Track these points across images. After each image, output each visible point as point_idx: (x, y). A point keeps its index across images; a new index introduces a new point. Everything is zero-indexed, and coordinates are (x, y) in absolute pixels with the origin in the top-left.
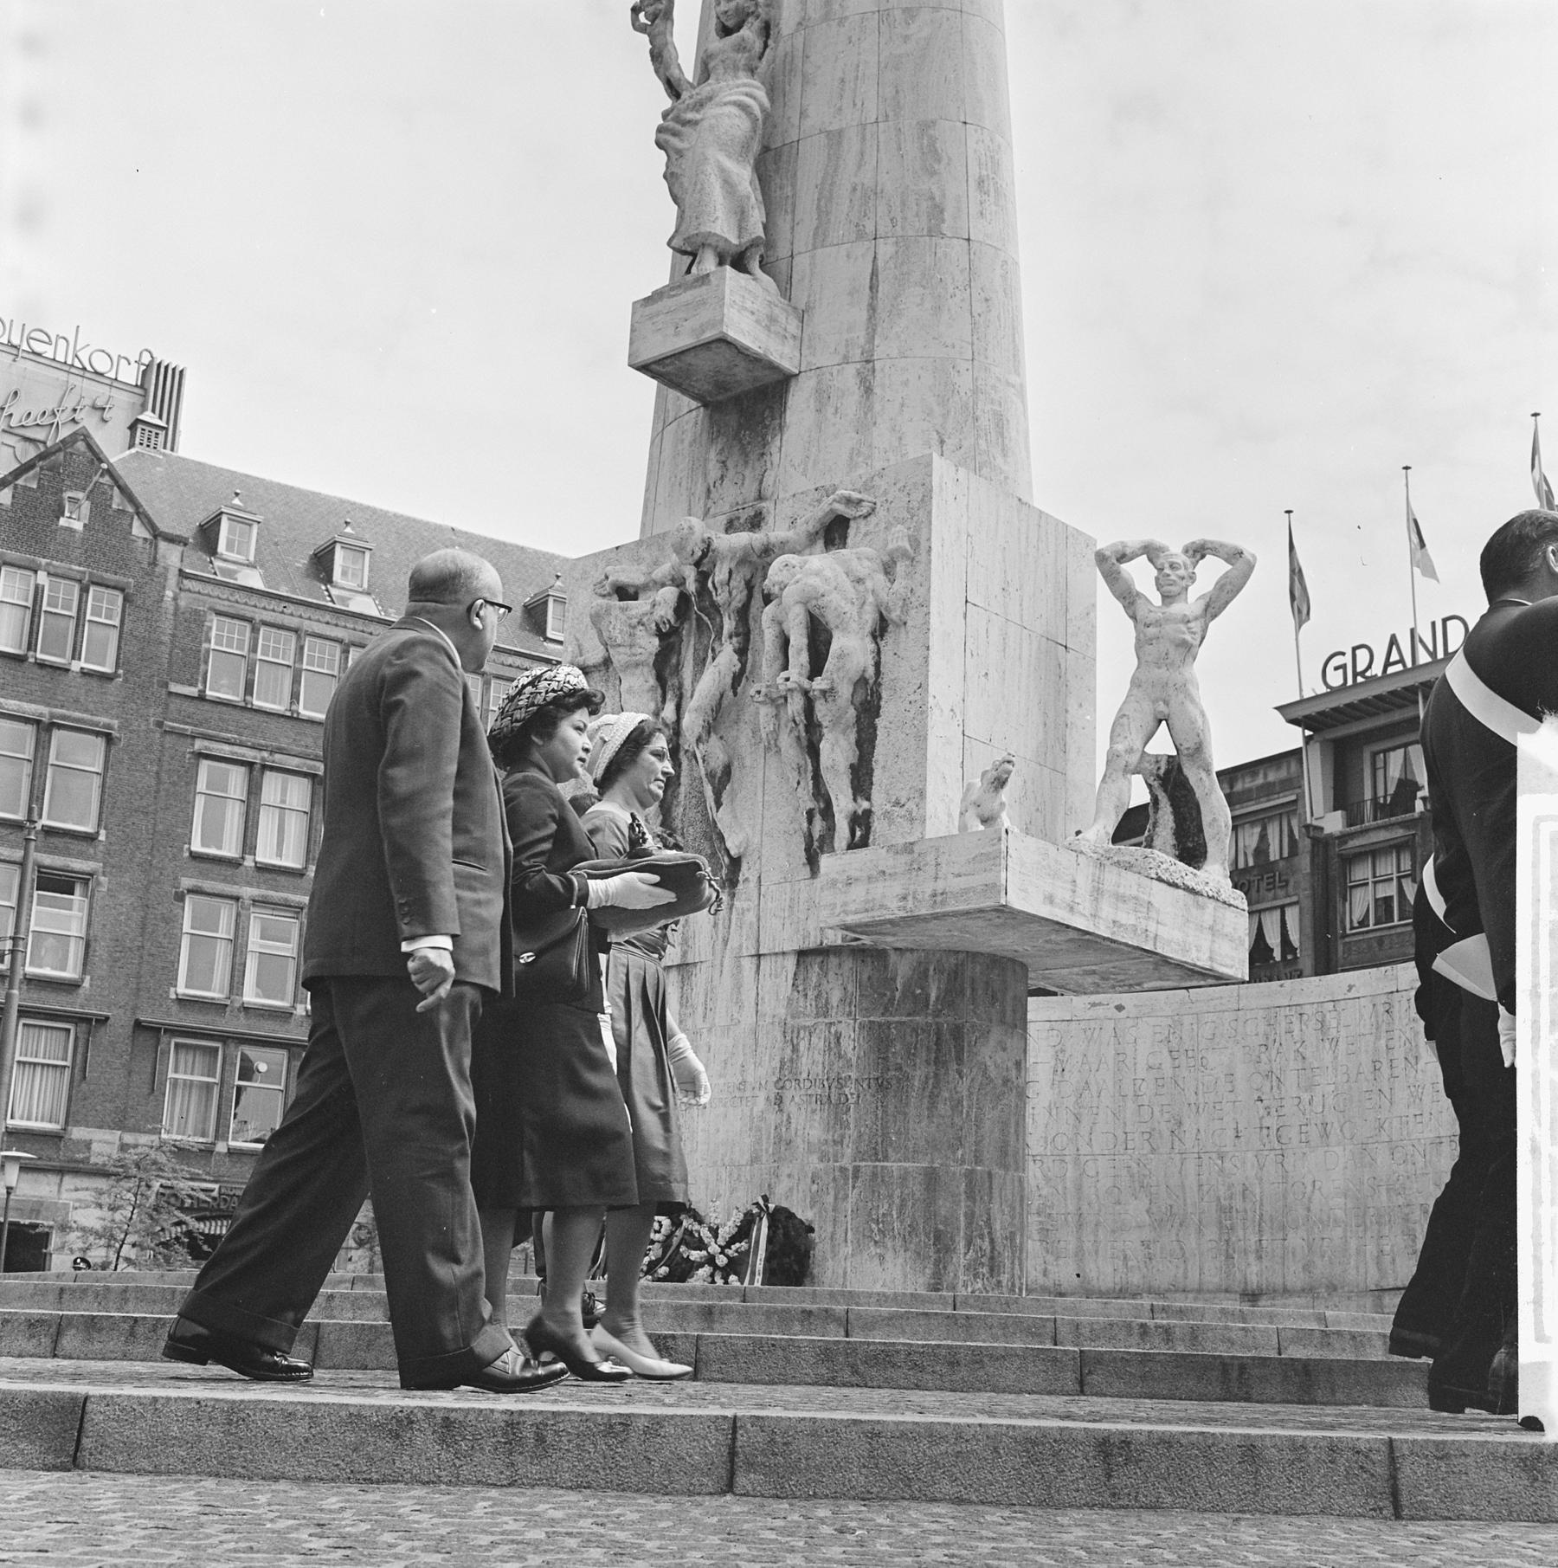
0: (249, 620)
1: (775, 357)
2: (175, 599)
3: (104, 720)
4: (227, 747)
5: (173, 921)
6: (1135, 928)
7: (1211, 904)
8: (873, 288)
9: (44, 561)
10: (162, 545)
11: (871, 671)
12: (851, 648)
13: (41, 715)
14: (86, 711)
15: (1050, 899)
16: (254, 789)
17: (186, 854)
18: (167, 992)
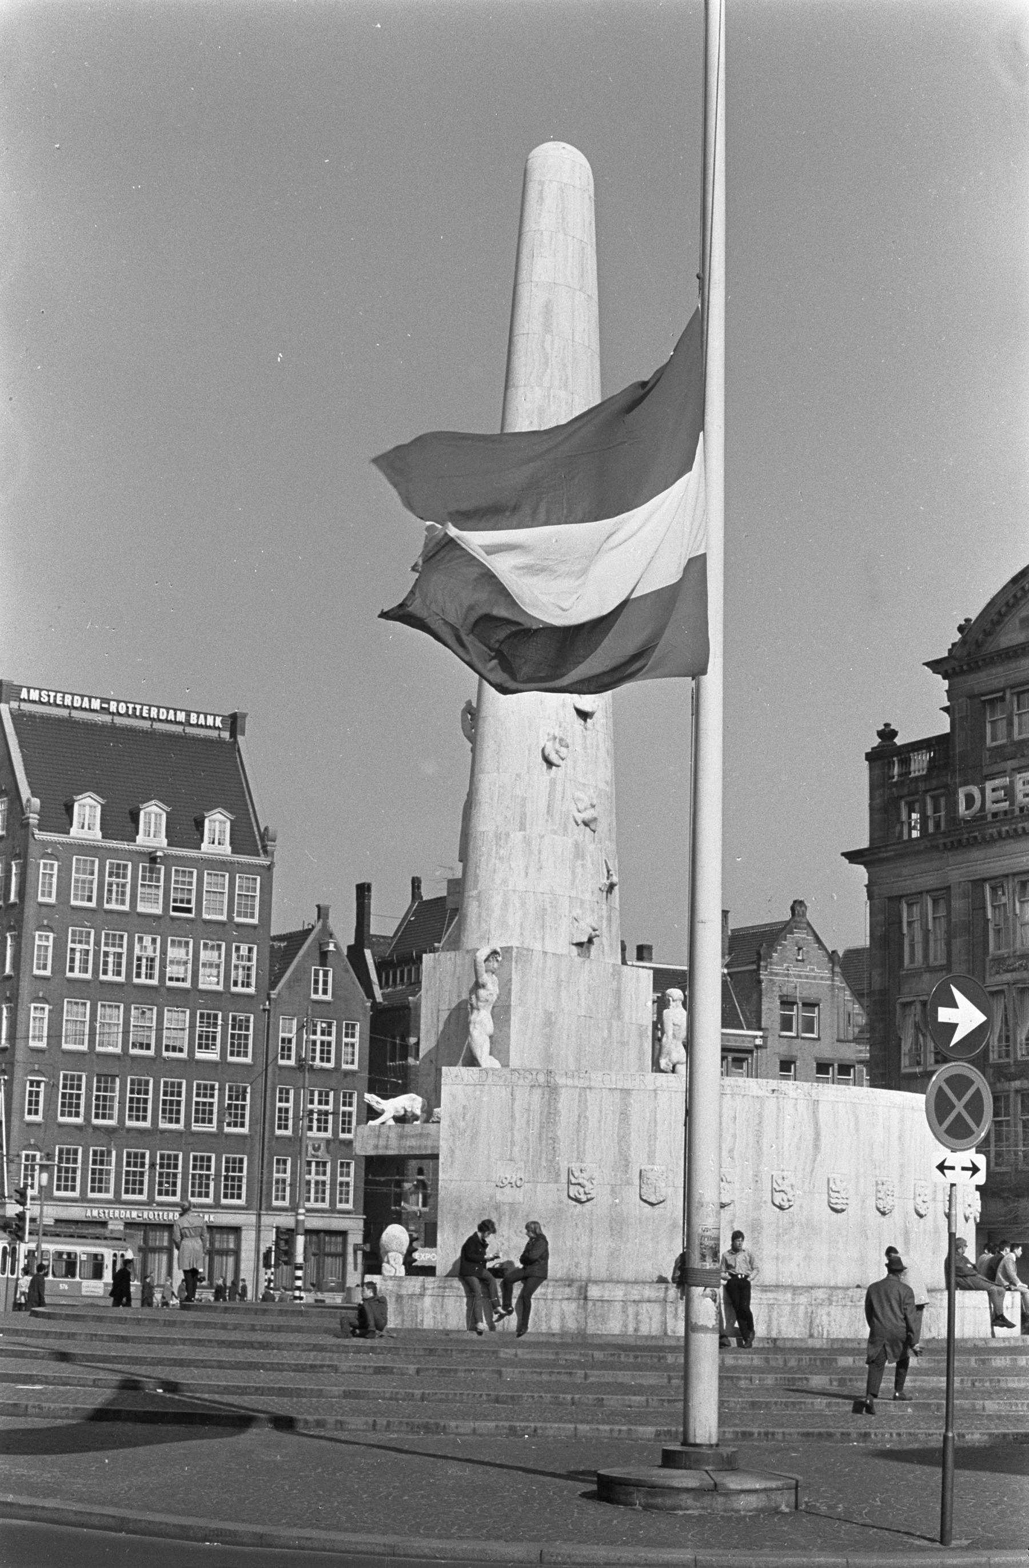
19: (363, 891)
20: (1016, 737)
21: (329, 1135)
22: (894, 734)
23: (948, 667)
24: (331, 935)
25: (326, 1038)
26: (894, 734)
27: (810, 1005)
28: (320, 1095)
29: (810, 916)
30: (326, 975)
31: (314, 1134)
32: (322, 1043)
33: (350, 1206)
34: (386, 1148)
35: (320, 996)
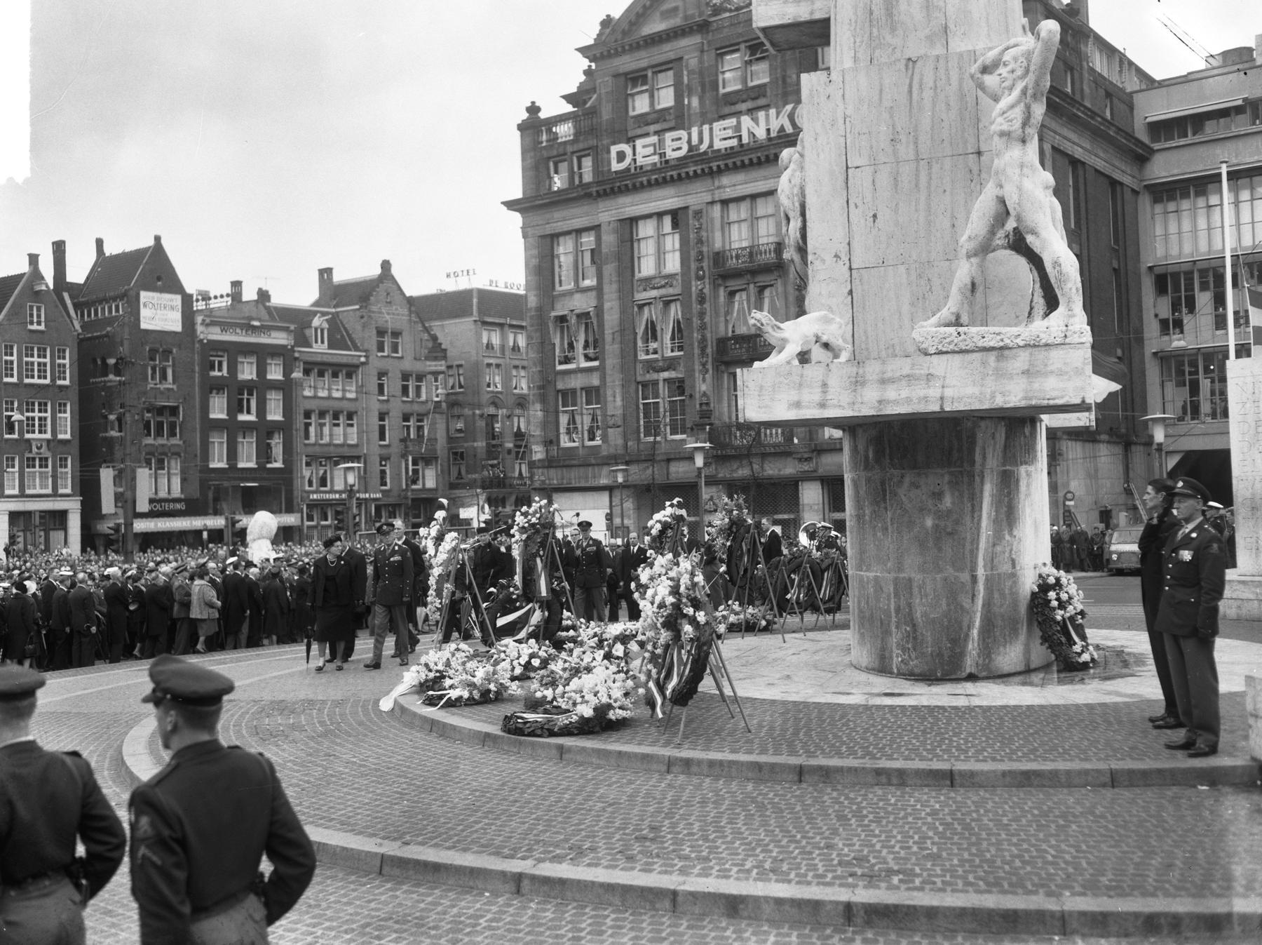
6: (908, 400)
7: (1024, 356)
15: (798, 405)
19: (59, 249)
20: (658, 107)
21: (48, 436)
22: (539, 109)
23: (597, 52)
24: (43, 278)
25: (42, 360)
26: (539, 109)
27: (396, 334)
28: (40, 404)
29: (395, 271)
30: (39, 309)
31: (37, 435)
32: (39, 364)
33: (68, 491)
34: (822, 405)
35: (35, 327)
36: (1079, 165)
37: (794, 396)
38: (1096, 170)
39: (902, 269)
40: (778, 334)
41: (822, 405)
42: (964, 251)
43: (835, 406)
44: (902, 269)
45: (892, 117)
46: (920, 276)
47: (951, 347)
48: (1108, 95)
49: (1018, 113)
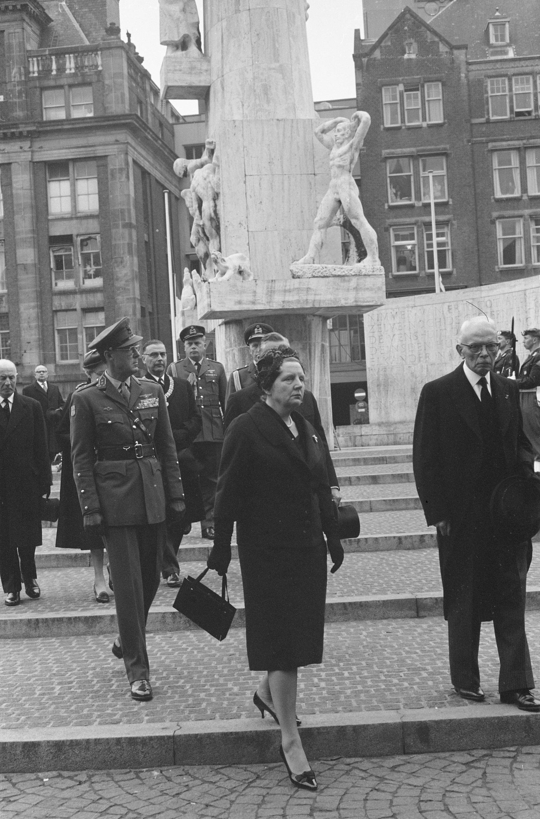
0: (505, 75)
1: (196, 83)
2: (467, 77)
3: (442, 146)
4: (504, 143)
5: (492, 234)
6: (298, 301)
7: (354, 280)
8: (222, 42)
9: (401, 79)
10: (456, 52)
11: (213, 214)
12: (208, 206)
13: (413, 152)
14: (433, 144)
15: (240, 302)
16: (523, 162)
17: (493, 201)
18: (494, 269)
36: (147, 176)
37: (237, 298)
38: (156, 180)
39: (276, 233)
40: (223, 264)
41: (253, 303)
42: (317, 225)
43: (259, 303)
44: (276, 233)
45: (269, 150)
46: (285, 238)
47: (320, 274)
48: (161, 125)
49: (348, 157)
